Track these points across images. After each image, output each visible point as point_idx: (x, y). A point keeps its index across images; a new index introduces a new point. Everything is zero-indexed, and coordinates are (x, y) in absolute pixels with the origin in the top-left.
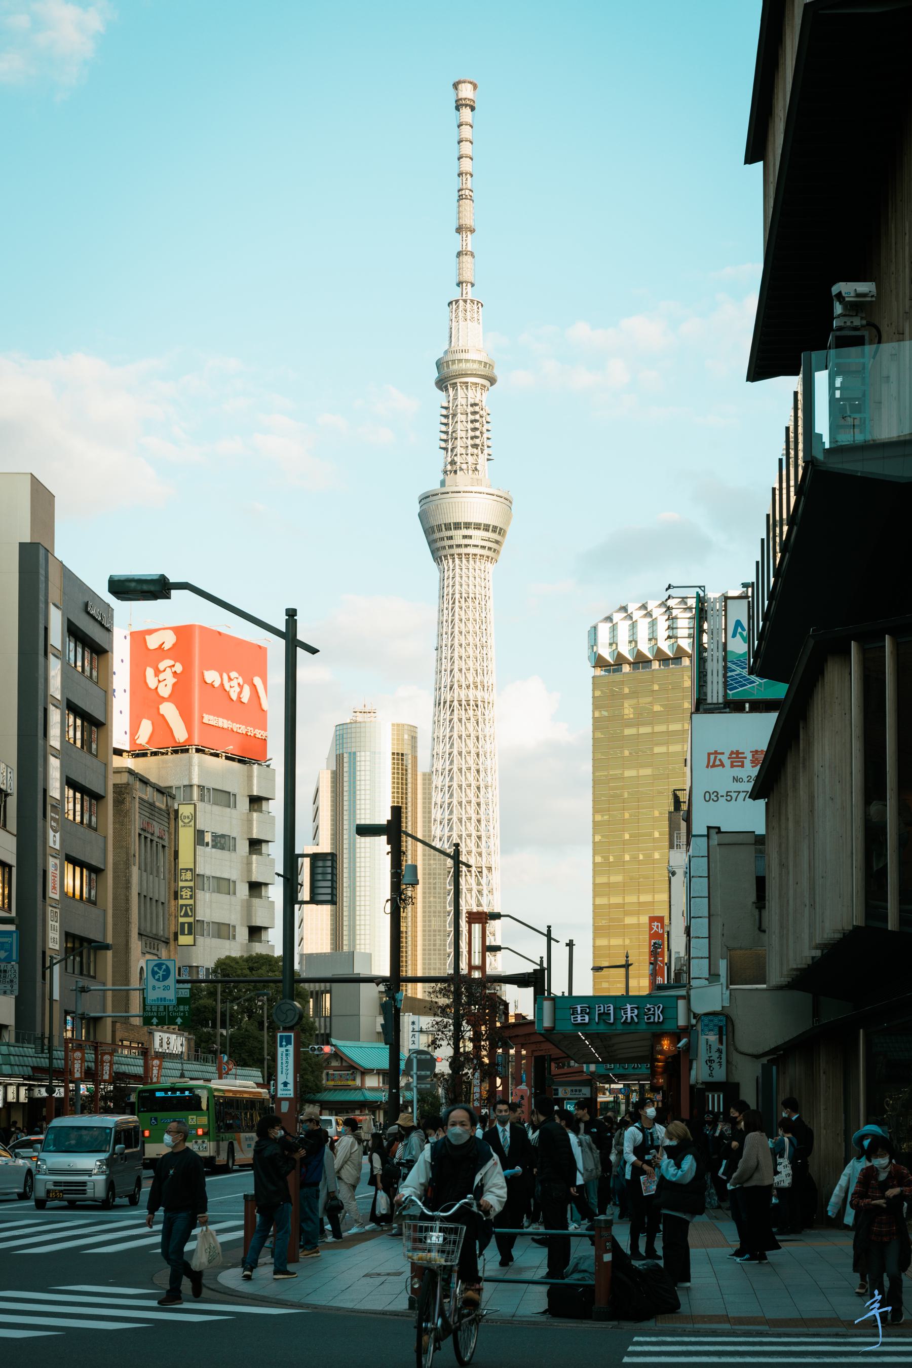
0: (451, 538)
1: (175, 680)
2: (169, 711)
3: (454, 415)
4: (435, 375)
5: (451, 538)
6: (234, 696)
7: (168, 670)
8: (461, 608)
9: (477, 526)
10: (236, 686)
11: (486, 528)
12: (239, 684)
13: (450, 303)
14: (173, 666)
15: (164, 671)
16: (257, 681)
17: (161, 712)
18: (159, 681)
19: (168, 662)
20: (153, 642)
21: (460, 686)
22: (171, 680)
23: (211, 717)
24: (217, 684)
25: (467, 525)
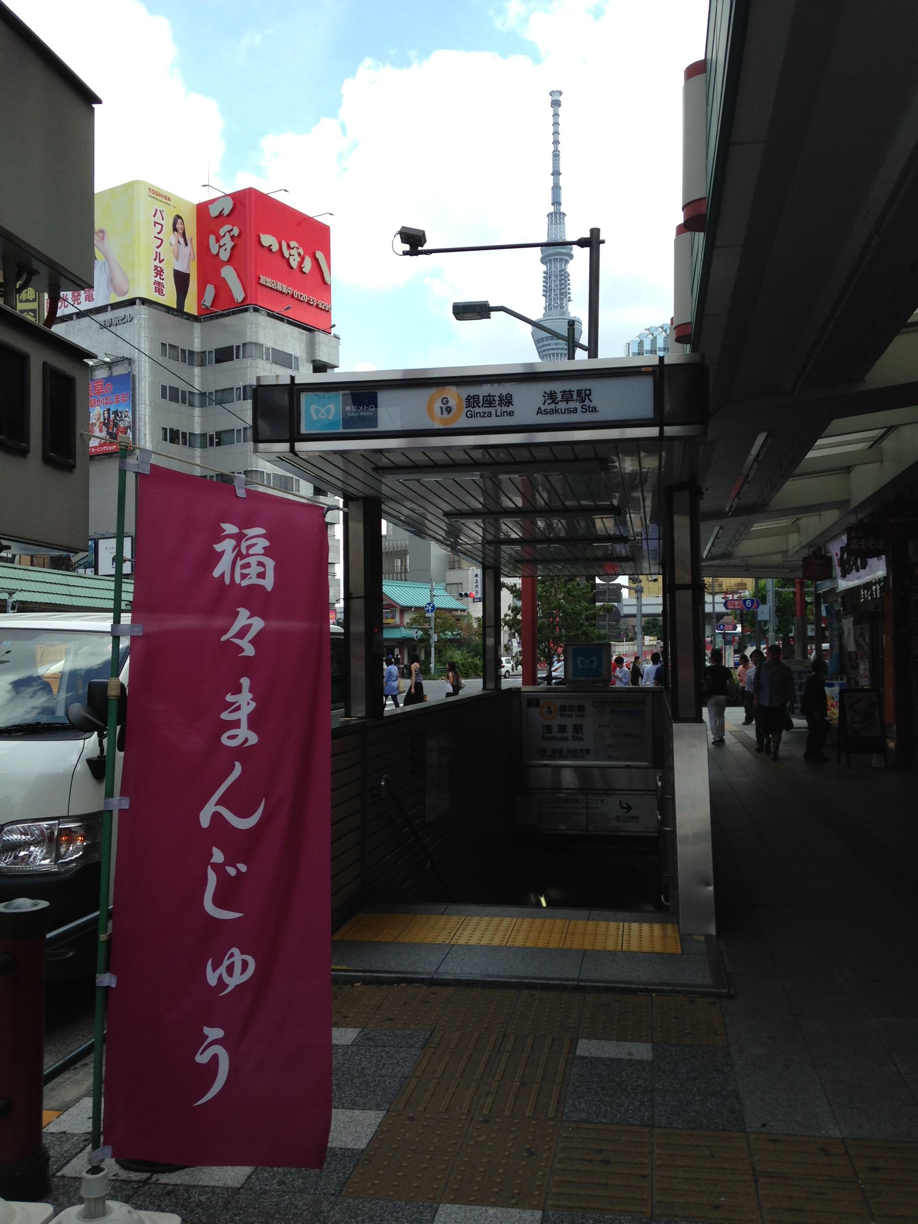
0: (549, 345)
1: (233, 244)
2: (229, 274)
3: (550, 277)
5: (549, 345)
6: (294, 264)
7: (228, 234)
10: (296, 255)
12: (299, 254)
13: (548, 215)
14: (232, 230)
15: (224, 236)
16: (320, 255)
17: (223, 275)
18: (220, 247)
19: (228, 227)
20: (214, 211)
22: (230, 244)
23: (269, 280)
24: (275, 248)
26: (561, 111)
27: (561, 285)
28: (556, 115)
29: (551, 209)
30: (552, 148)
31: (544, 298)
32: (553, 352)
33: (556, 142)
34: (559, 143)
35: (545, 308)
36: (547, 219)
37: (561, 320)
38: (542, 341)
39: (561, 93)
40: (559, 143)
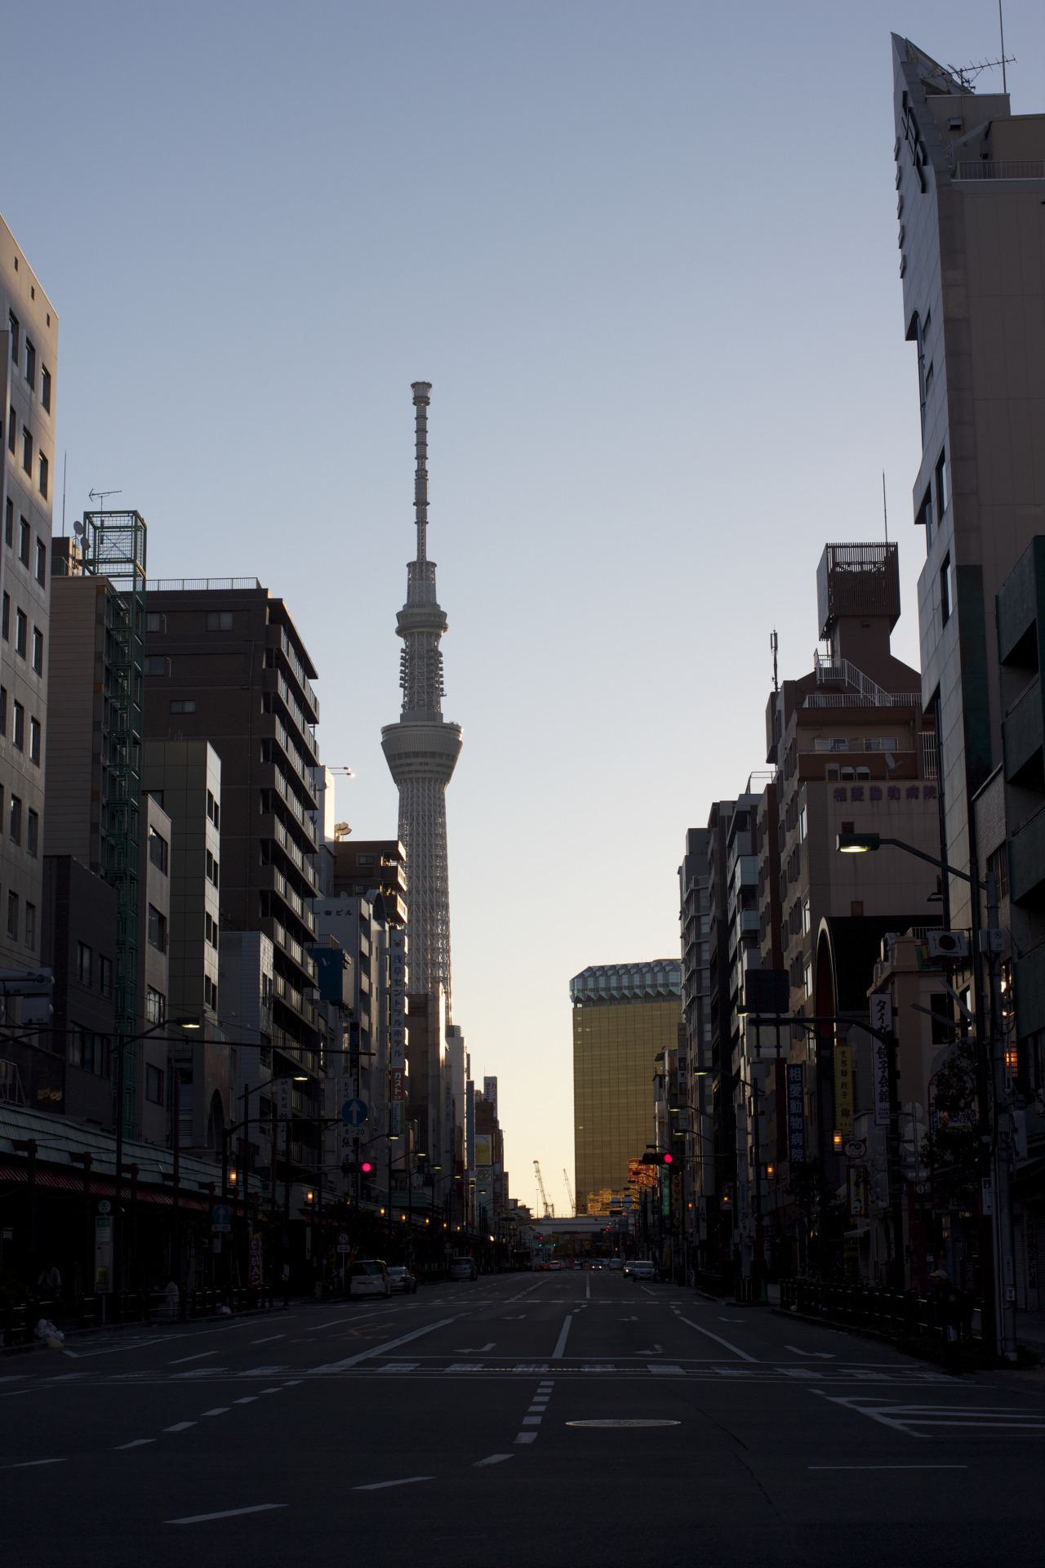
0: (410, 764)
4: (396, 625)
5: (410, 764)
8: (418, 823)
9: (433, 755)
11: (441, 755)
21: (418, 892)
25: (425, 754)
26: (430, 411)
27: (430, 672)
28: (421, 418)
29: (414, 558)
30: (414, 465)
31: (402, 689)
32: (419, 775)
33: (421, 457)
34: (427, 458)
35: (403, 706)
36: (407, 569)
37: (432, 729)
38: (400, 758)
39: (429, 385)
40: (427, 458)
